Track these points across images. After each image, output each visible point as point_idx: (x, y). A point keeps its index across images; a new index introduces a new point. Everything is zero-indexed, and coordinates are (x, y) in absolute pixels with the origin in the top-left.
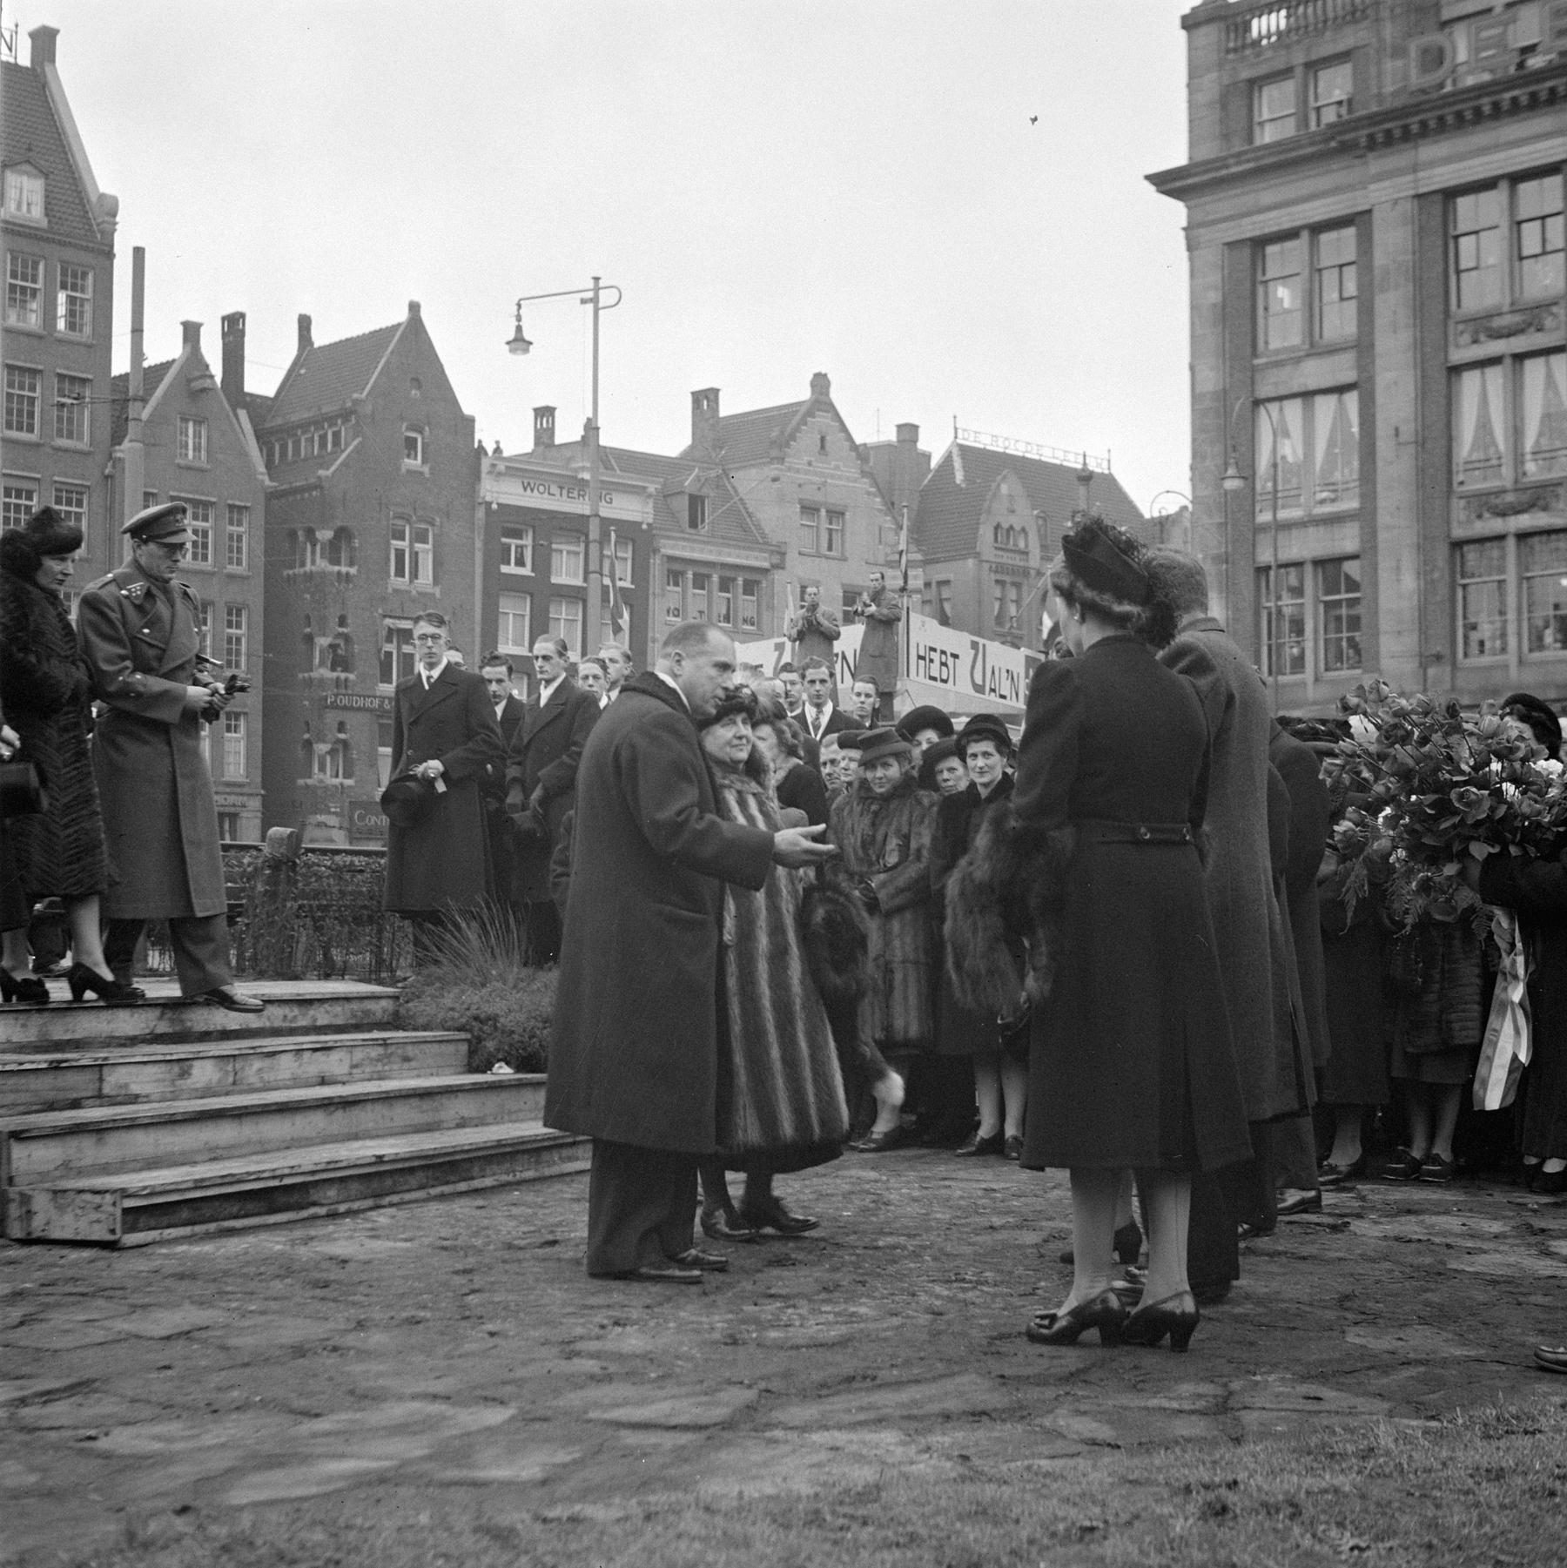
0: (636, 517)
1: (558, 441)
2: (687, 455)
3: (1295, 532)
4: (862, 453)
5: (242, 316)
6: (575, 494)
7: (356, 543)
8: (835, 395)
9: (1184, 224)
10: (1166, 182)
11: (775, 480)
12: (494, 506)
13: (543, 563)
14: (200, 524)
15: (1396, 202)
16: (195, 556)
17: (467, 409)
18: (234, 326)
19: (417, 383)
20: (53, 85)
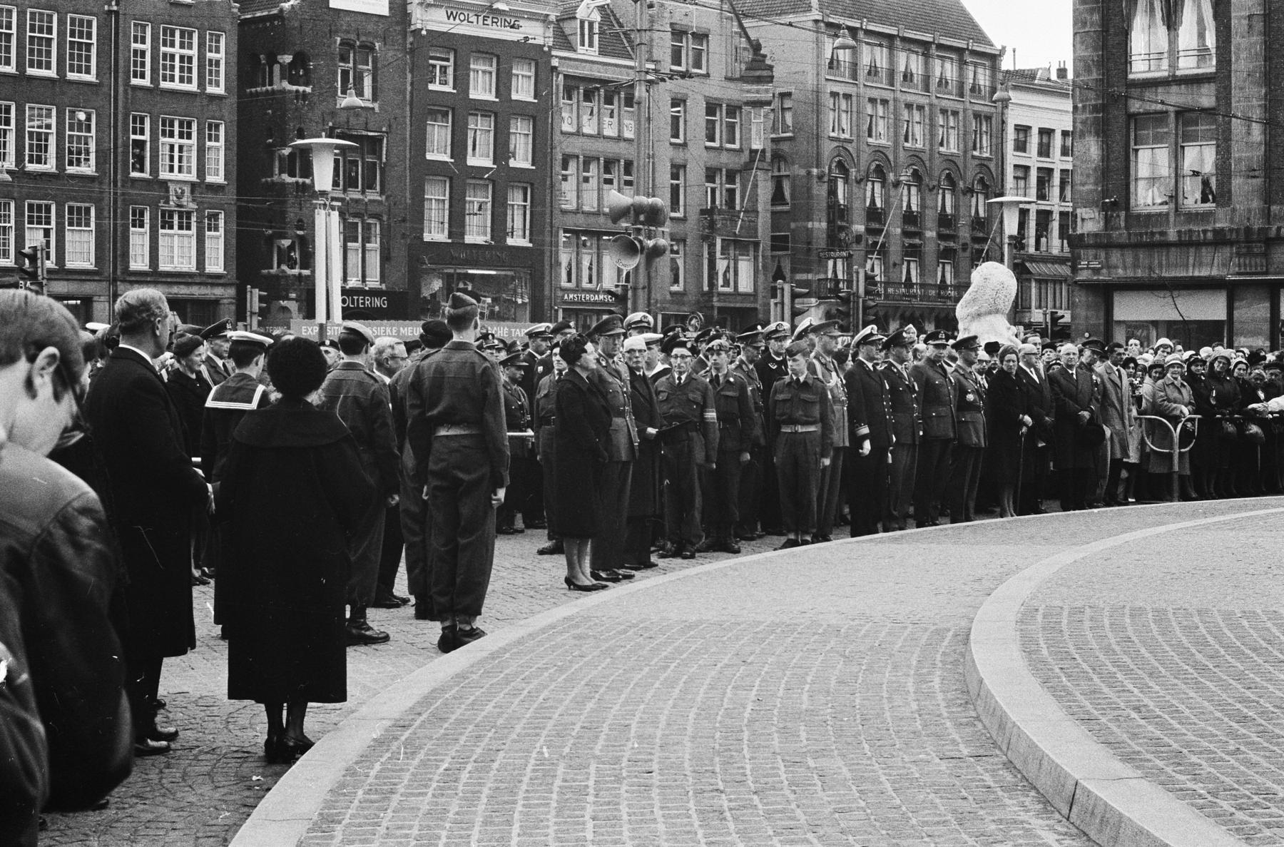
6: (489, 21)
12: (424, 32)
13: (462, 82)
14: (186, 52)
16: (182, 80)
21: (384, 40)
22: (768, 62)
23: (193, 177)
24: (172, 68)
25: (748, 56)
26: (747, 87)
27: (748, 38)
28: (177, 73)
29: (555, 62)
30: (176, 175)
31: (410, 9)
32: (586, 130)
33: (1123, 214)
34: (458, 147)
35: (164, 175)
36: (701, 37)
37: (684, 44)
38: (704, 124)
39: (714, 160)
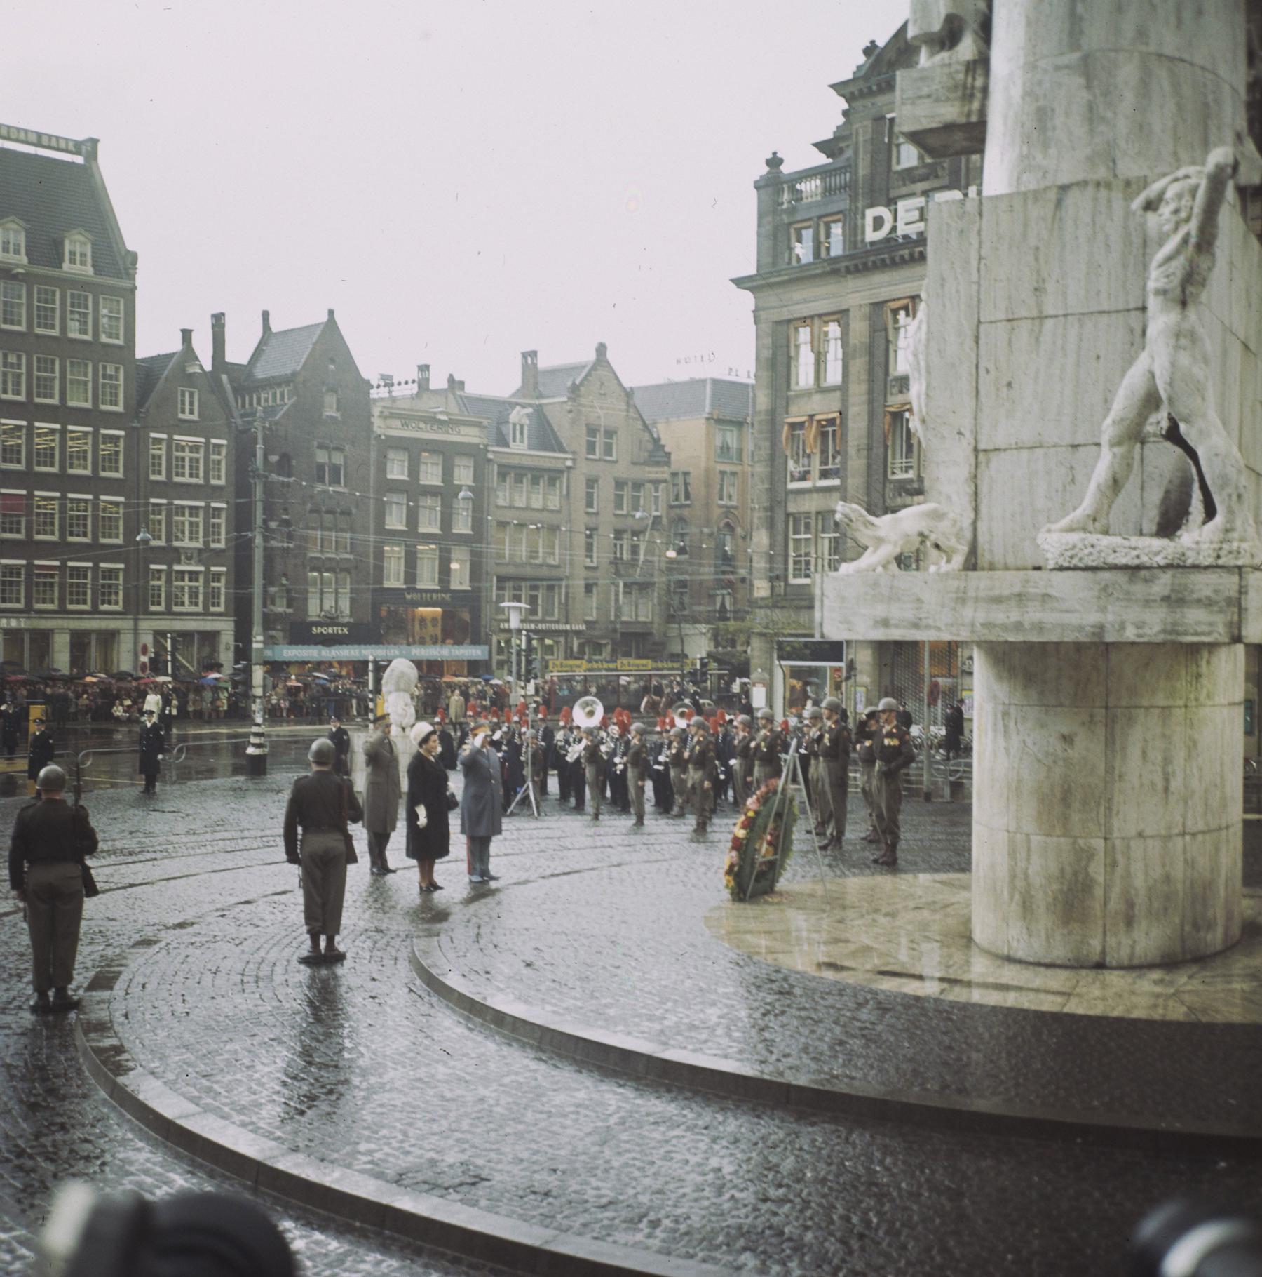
0: (476, 440)
1: (432, 386)
3: (807, 496)
4: (629, 394)
5: (223, 314)
6: (435, 427)
7: (294, 463)
8: (610, 356)
10: (739, 282)
11: (570, 412)
13: (414, 472)
15: (861, 306)
16: (191, 475)
17: (365, 374)
18: (218, 321)
19: (332, 361)
20: (96, 174)
21: (353, 443)
22: (667, 449)
23: (200, 545)
24: (183, 467)
25: (650, 446)
26: (647, 469)
28: (187, 471)
29: (490, 456)
30: (186, 543)
32: (517, 504)
33: (782, 584)
34: (412, 519)
35: (176, 544)
36: (610, 433)
37: (597, 439)
38: (612, 497)
39: (620, 526)
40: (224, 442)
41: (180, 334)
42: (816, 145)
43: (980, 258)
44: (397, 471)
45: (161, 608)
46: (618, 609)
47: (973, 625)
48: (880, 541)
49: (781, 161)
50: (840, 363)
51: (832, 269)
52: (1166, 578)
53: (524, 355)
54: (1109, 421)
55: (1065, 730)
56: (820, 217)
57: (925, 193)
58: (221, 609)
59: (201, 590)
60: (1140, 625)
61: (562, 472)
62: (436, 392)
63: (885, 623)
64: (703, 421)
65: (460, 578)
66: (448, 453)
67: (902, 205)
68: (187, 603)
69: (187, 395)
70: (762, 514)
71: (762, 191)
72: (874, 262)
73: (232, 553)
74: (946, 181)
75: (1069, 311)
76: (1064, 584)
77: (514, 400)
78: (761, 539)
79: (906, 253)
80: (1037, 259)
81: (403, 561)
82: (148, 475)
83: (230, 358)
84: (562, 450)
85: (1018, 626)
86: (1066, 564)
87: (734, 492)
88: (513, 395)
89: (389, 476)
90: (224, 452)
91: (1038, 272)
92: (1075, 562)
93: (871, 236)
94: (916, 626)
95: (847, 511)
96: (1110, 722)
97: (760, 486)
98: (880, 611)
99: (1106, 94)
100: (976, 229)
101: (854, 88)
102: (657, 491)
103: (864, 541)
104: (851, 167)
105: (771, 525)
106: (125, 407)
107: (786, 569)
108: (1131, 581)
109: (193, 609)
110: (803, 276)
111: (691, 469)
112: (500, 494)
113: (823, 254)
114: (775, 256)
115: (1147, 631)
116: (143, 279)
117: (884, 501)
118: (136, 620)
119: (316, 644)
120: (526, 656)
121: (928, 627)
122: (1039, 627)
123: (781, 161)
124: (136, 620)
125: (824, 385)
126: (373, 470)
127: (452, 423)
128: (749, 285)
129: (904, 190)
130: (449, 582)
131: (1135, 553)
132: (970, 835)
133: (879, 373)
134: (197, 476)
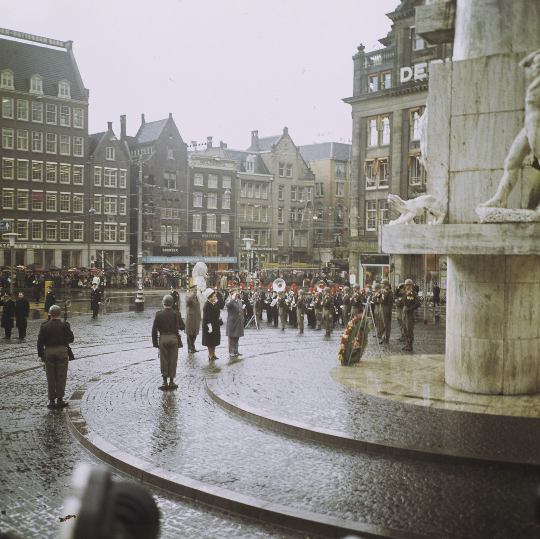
1: (213, 146)
2: (250, 149)
3: (374, 193)
4: (297, 149)
5: (125, 115)
6: (215, 164)
7: (155, 179)
8: (289, 132)
9: (352, 112)
10: (345, 100)
13: (206, 183)
15: (398, 110)
16: (112, 184)
17: (185, 141)
18: (123, 119)
19: (171, 135)
22: (314, 173)
23: (115, 214)
24: (108, 181)
25: (306, 172)
26: (306, 181)
27: (307, 166)
28: (110, 182)
29: (238, 176)
30: (109, 213)
31: (188, 160)
33: (363, 231)
34: (205, 203)
35: (105, 213)
36: (289, 166)
38: (290, 194)
39: (294, 205)
40: (126, 170)
41: (107, 124)
42: (379, 40)
43: (452, 88)
44: (198, 182)
45: (99, 241)
46: (292, 241)
47: (447, 247)
48: (407, 211)
49: (364, 47)
50: (389, 136)
51: (385, 94)
52: (532, 227)
53: (253, 132)
54: (507, 159)
55: (487, 293)
56: (381, 72)
57: (427, 61)
58: (124, 241)
59: (116, 233)
60: (520, 247)
61: (268, 183)
62: (215, 148)
63: (409, 246)
64: (329, 162)
65: (225, 229)
66: (220, 174)
67: (416, 66)
68: (110, 238)
69: (110, 150)
70: (355, 200)
71: (356, 61)
72: (404, 91)
73: (128, 217)
74: (436, 56)
75: (491, 111)
76: (487, 230)
77: (248, 152)
78: (354, 211)
79: (418, 87)
80: (477, 88)
81: (201, 221)
82: (93, 184)
83: (128, 134)
84: (269, 173)
85: (467, 248)
86: (488, 221)
87: (342, 191)
88: (248, 150)
89: (195, 185)
90: (125, 174)
91: (477, 94)
92: (492, 220)
93: (403, 80)
94: (422, 248)
95: (393, 198)
96: (507, 290)
97: (354, 189)
98: (407, 241)
99: (508, 15)
100: (450, 75)
101: (396, 16)
102: (309, 191)
103: (401, 211)
104: (394, 50)
105: (358, 206)
106: (84, 155)
107: (365, 224)
108: (517, 228)
109: (113, 241)
110: (373, 97)
111: (324, 182)
112: (242, 192)
113: (382, 88)
114: (361, 89)
115: (523, 250)
116: (91, 101)
117: (408, 194)
118: (89, 245)
119: (164, 256)
120: (253, 261)
121: (427, 248)
122: (476, 248)
123: (364, 47)
124: (89, 245)
125: (382, 145)
126: (188, 182)
127: (222, 162)
128: (349, 101)
129: (417, 60)
130: (220, 229)
131: (518, 216)
132: (444, 338)
133: (407, 138)
134: (114, 184)
